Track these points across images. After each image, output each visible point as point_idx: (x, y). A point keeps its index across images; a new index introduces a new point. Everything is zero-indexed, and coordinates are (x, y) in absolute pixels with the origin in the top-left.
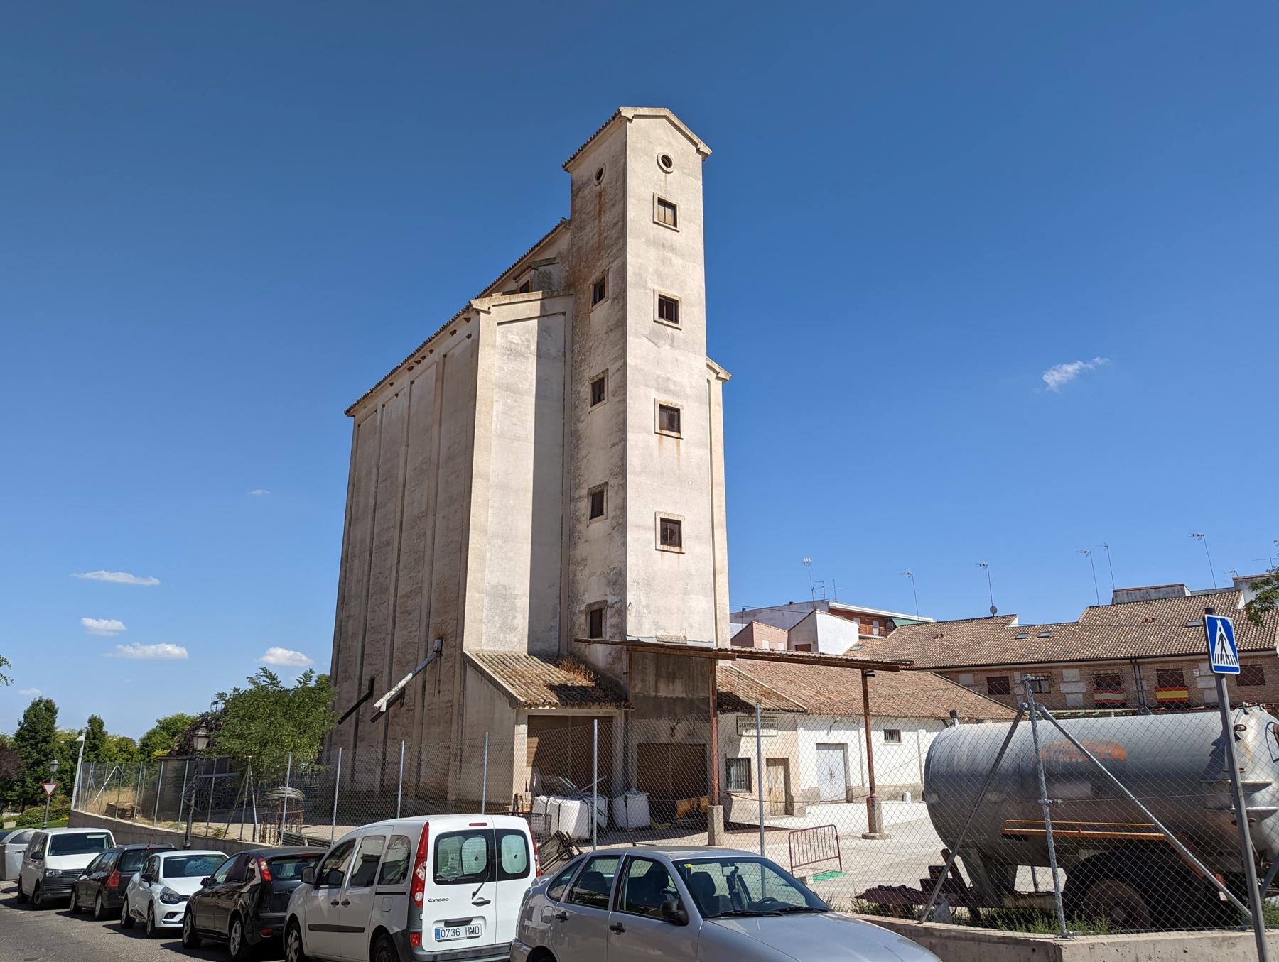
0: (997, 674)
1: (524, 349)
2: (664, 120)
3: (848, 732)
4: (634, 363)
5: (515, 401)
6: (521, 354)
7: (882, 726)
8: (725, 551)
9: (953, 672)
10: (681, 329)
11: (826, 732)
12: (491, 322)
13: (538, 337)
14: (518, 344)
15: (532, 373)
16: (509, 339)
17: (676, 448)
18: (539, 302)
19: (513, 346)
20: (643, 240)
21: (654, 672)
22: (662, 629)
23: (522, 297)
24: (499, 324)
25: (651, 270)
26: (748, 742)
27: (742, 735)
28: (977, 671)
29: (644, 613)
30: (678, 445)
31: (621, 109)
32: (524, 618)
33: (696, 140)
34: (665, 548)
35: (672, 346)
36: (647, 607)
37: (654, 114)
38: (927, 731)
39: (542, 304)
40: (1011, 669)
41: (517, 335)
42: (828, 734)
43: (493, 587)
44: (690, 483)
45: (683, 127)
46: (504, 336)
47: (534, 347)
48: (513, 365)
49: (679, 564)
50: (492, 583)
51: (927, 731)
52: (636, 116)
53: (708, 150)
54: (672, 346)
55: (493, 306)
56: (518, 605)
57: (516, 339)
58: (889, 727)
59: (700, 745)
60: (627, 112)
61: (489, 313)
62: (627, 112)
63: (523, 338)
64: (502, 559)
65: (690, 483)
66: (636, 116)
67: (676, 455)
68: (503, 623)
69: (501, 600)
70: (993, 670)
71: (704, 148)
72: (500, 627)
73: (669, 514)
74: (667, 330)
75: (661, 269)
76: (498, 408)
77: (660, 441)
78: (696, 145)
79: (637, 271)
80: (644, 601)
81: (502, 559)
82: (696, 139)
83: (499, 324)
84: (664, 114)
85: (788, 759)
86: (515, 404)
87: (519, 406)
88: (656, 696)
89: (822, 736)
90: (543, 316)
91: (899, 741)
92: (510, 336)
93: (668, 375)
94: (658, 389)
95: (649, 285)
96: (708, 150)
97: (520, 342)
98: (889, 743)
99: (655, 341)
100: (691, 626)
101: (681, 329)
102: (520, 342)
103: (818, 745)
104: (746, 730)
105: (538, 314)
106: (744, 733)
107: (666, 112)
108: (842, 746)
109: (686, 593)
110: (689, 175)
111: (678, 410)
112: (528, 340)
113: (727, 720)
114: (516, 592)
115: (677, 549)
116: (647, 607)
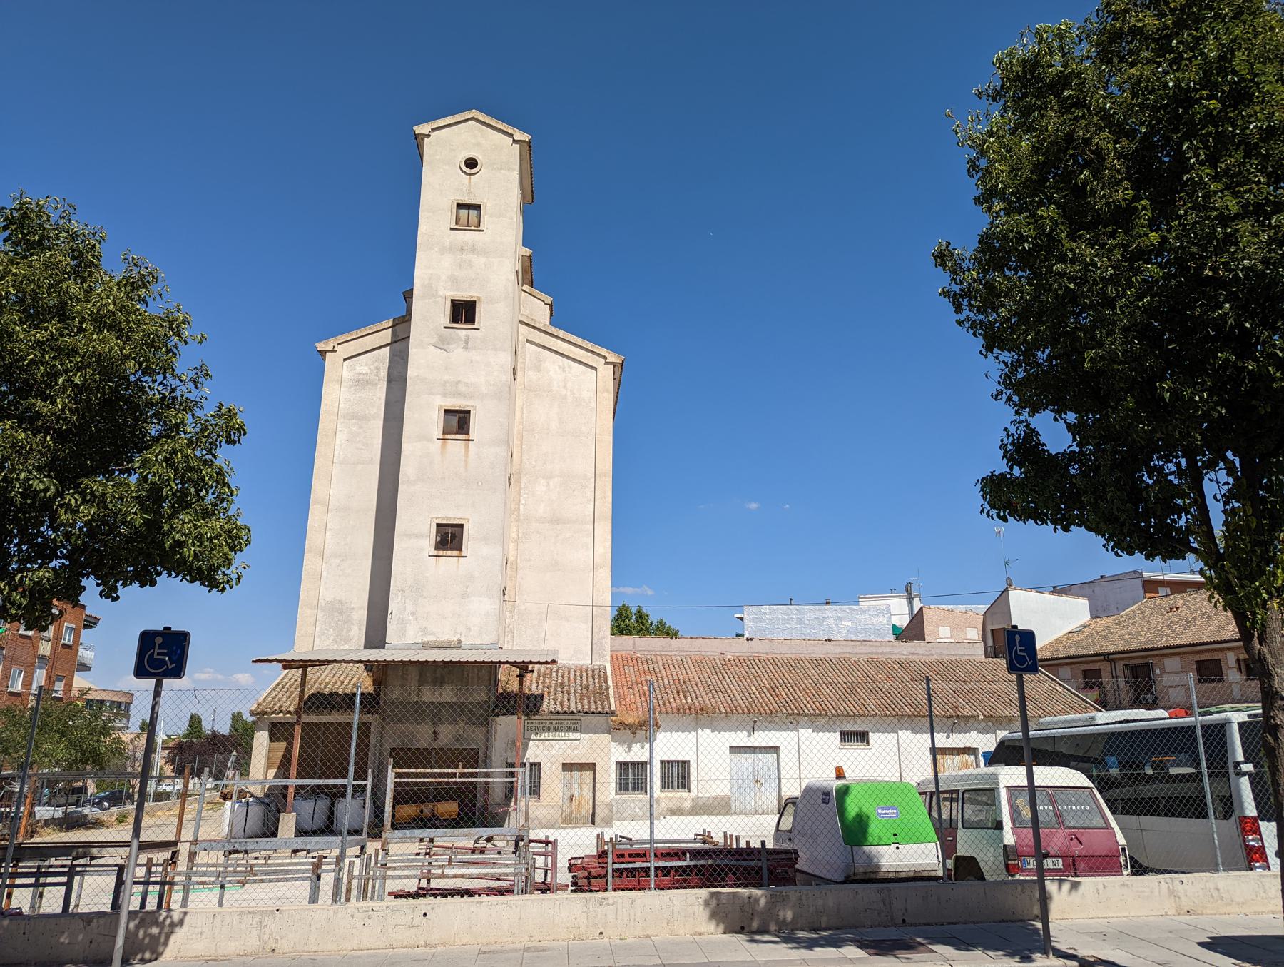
0: (1207, 657)
1: (372, 377)
2: (472, 122)
3: (785, 734)
4: (416, 374)
5: (361, 427)
6: (370, 383)
7: (839, 729)
8: (609, 544)
9: (1157, 655)
10: (478, 329)
11: (745, 733)
12: (337, 359)
13: (390, 362)
14: (367, 374)
15: (380, 398)
16: (357, 371)
17: (463, 451)
18: (390, 329)
19: (361, 377)
20: (436, 249)
21: (418, 677)
22: (430, 634)
23: (370, 329)
24: (345, 360)
25: (444, 277)
26: (538, 746)
27: (530, 740)
28: (1184, 653)
29: (410, 620)
30: (467, 447)
31: (414, 128)
32: (360, 629)
33: (510, 131)
34: (440, 553)
35: (466, 348)
36: (413, 614)
37: (457, 120)
38: (813, 731)
39: (393, 331)
40: (1223, 649)
41: (366, 365)
42: (749, 736)
43: (328, 603)
44: (480, 484)
45: (494, 123)
46: (352, 369)
47: (384, 374)
48: (359, 394)
49: (458, 567)
50: (328, 599)
51: (813, 731)
52: (434, 130)
53: (526, 137)
54: (466, 348)
55: (339, 344)
56: (355, 617)
57: (364, 369)
58: (850, 727)
59: (472, 749)
60: (421, 129)
61: (336, 351)
62: (421, 129)
63: (372, 367)
64: (339, 576)
65: (480, 484)
66: (434, 130)
67: (463, 458)
68: (337, 636)
69: (336, 614)
70: (1202, 651)
71: (519, 135)
72: (334, 639)
73: (447, 519)
74: (462, 332)
75: (456, 274)
76: (341, 437)
77: (443, 447)
78: (511, 135)
79: (426, 283)
80: (409, 608)
81: (339, 576)
82: (510, 129)
83: (345, 360)
84: (470, 117)
85: (540, 764)
86: (361, 430)
87: (365, 432)
88: (417, 703)
89: (741, 738)
90: (396, 342)
91: (868, 744)
92: (358, 368)
93: (459, 379)
94: (444, 395)
95: (441, 293)
96: (526, 137)
97: (369, 371)
98: (853, 747)
99: (445, 347)
100: (469, 629)
101: (478, 329)
102: (369, 371)
103: (731, 747)
104: (536, 734)
105: (389, 341)
106: (533, 737)
107: (474, 113)
108: (775, 750)
109: (465, 596)
110: (501, 169)
111: (468, 412)
112: (378, 368)
113: (507, 725)
114: (352, 606)
115: (455, 553)
116: (413, 614)
